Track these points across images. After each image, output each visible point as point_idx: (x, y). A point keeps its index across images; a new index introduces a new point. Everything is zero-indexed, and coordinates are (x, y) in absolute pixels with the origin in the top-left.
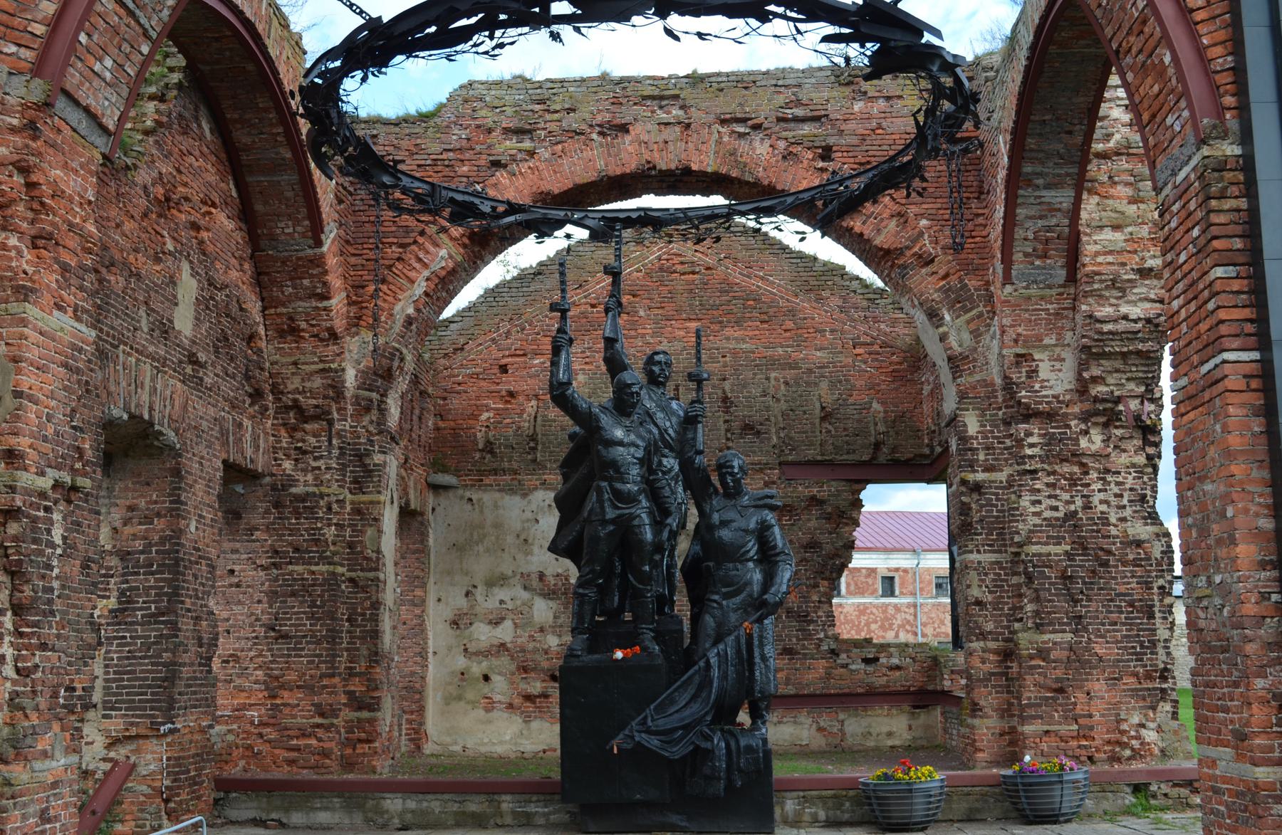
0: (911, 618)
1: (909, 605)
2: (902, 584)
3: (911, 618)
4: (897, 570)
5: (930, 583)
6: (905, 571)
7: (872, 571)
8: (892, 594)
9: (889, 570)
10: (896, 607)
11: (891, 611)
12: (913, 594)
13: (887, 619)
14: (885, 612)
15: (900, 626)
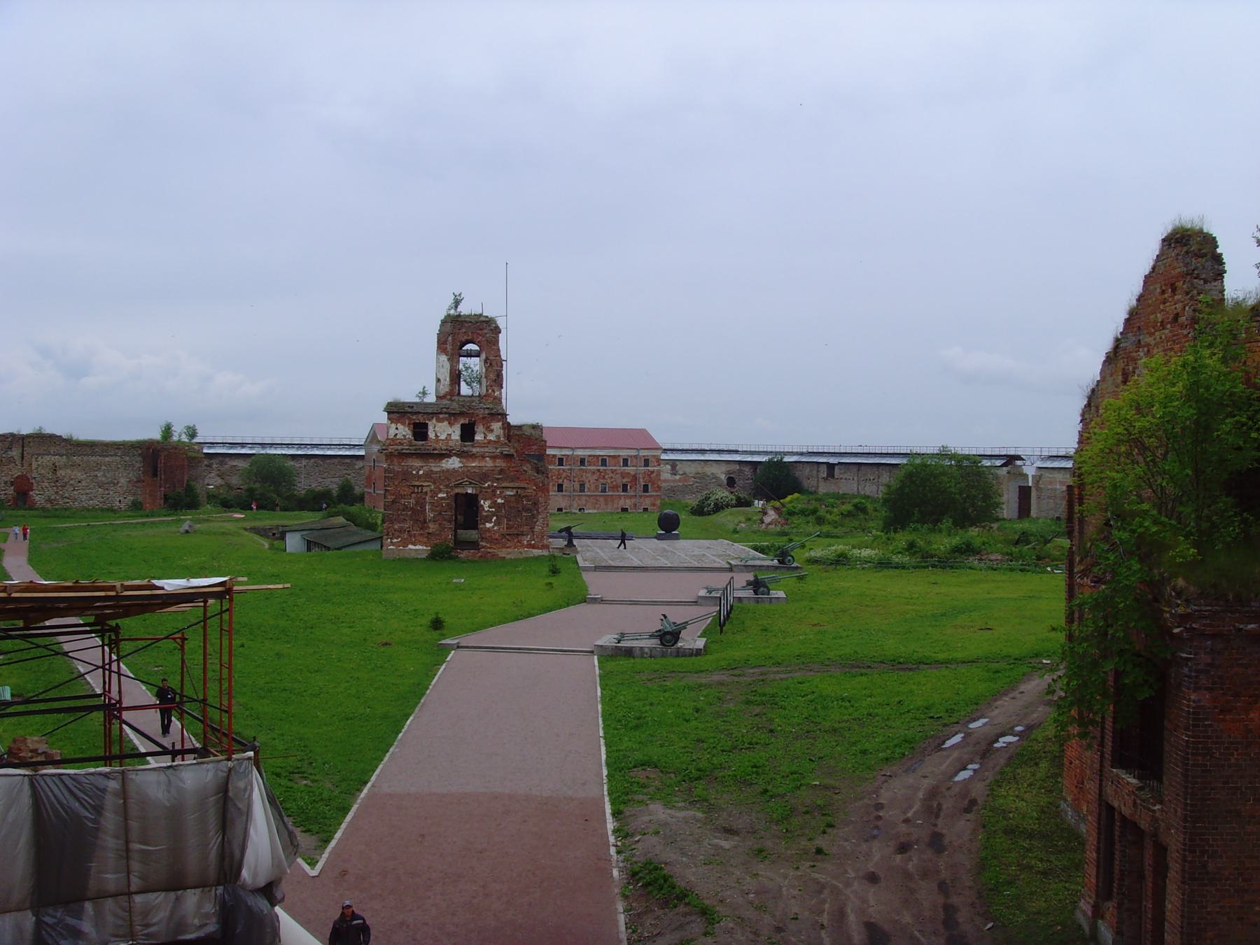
0: (569, 474)
1: (569, 469)
2: (566, 462)
3: (569, 474)
4: (564, 455)
5: (577, 461)
6: (568, 456)
7: (554, 456)
8: (562, 465)
9: (562, 455)
10: (563, 470)
11: (561, 471)
12: (570, 465)
13: (559, 475)
14: (559, 472)
15: (565, 478)
